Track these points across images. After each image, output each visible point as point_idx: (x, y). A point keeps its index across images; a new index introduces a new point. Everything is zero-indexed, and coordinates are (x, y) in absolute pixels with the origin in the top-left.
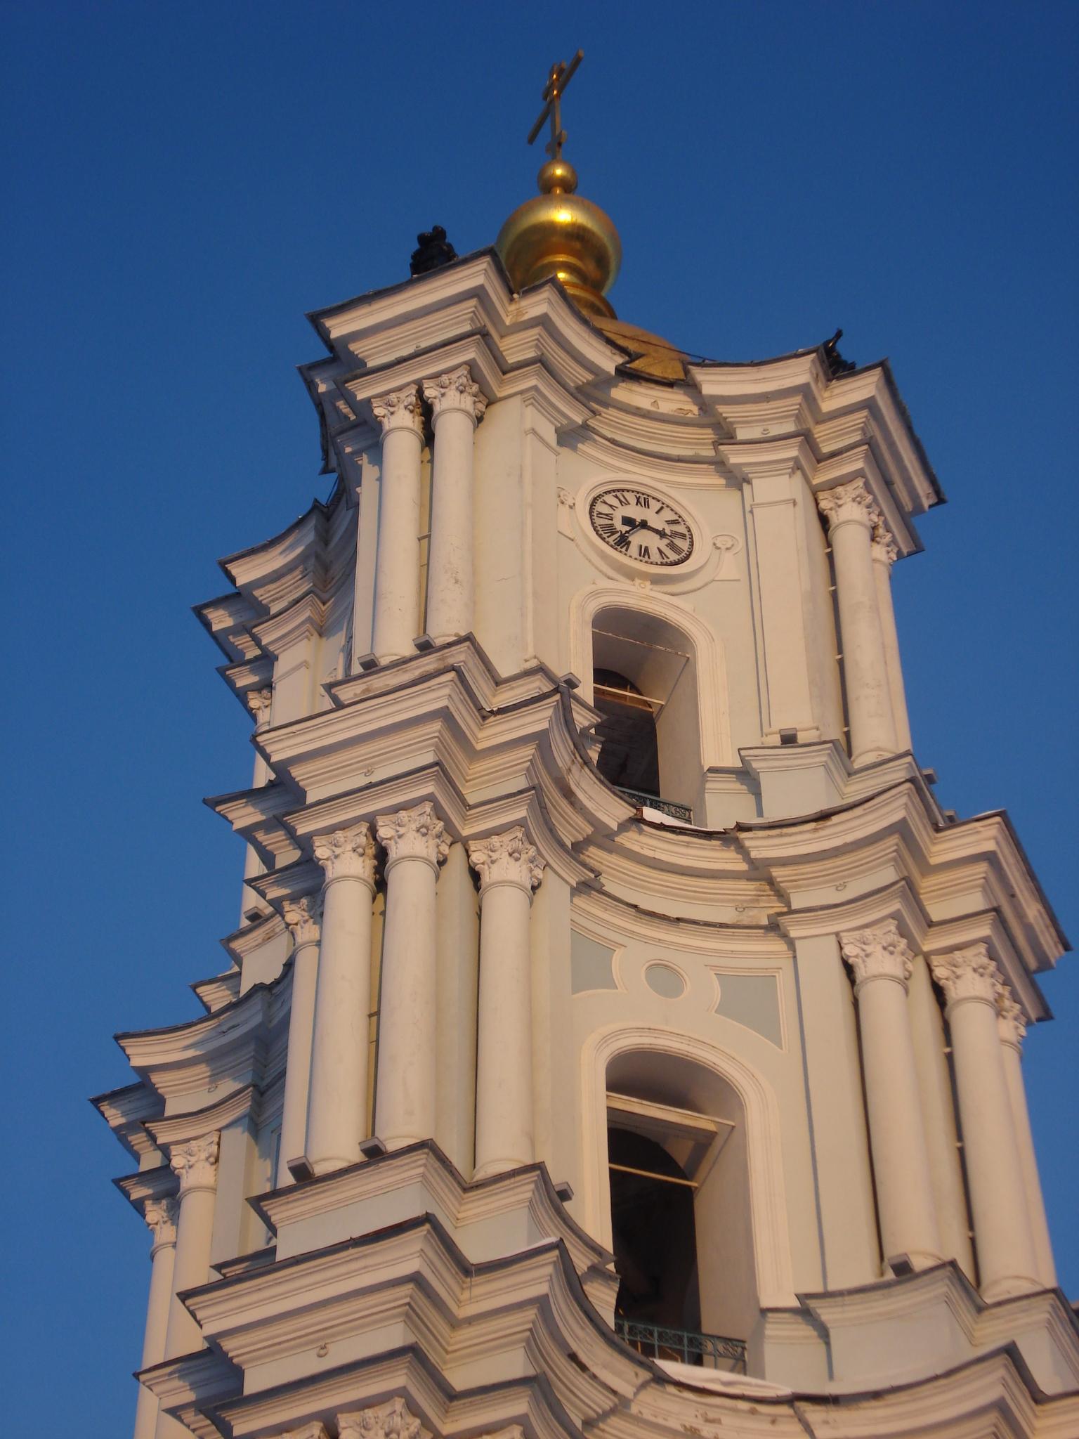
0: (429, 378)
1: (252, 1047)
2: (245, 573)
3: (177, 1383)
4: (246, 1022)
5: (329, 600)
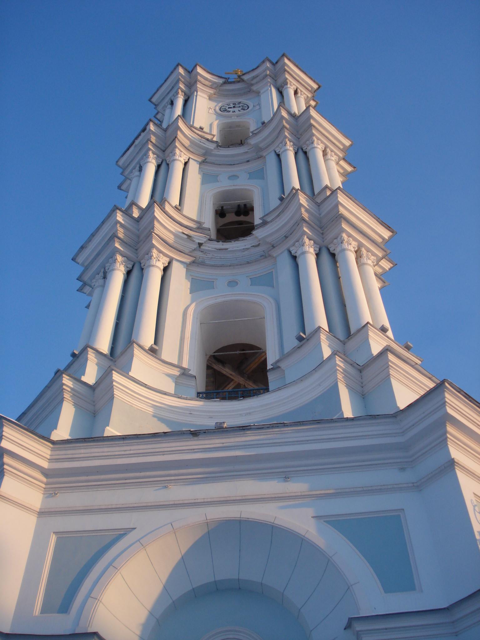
0: (300, 89)
1: (204, 151)
2: (199, 70)
3: (306, 202)
4: (208, 146)
5: (215, 95)
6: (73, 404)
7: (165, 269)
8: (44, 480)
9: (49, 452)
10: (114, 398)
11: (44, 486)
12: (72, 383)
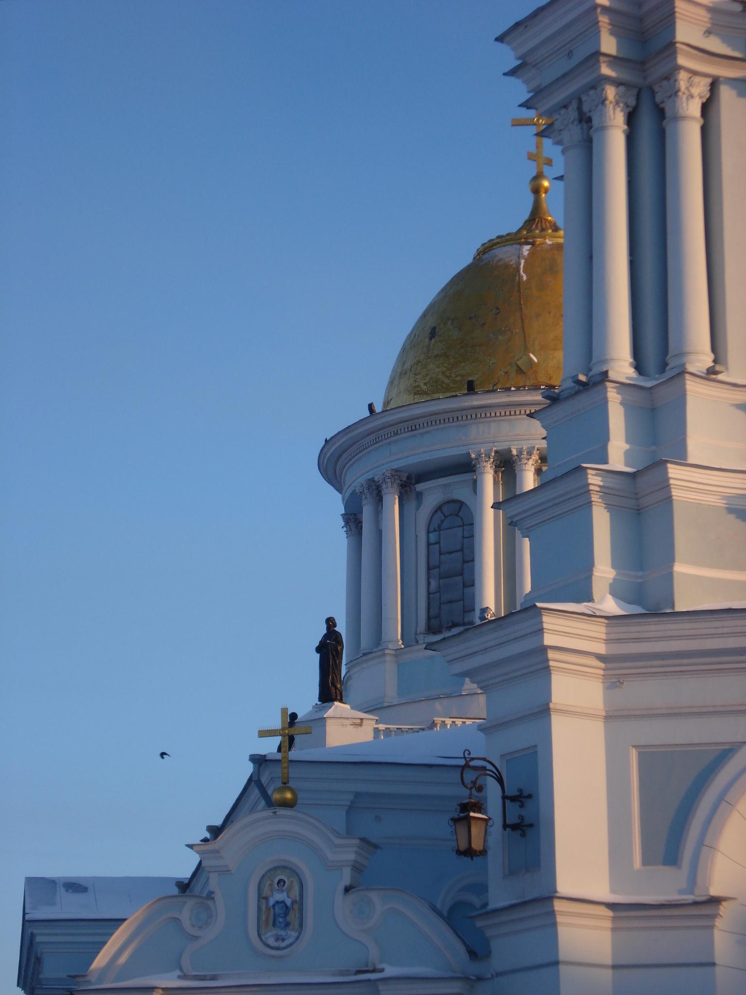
6: (605, 506)
7: (706, 108)
8: (602, 665)
9: (603, 629)
10: (674, 501)
11: (602, 672)
12: (600, 478)
